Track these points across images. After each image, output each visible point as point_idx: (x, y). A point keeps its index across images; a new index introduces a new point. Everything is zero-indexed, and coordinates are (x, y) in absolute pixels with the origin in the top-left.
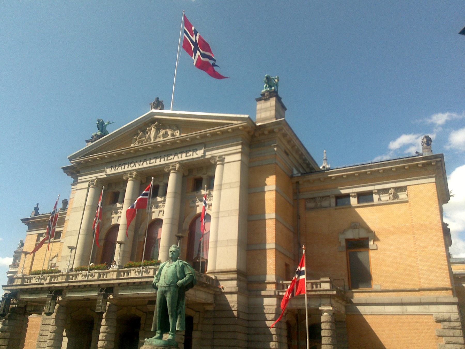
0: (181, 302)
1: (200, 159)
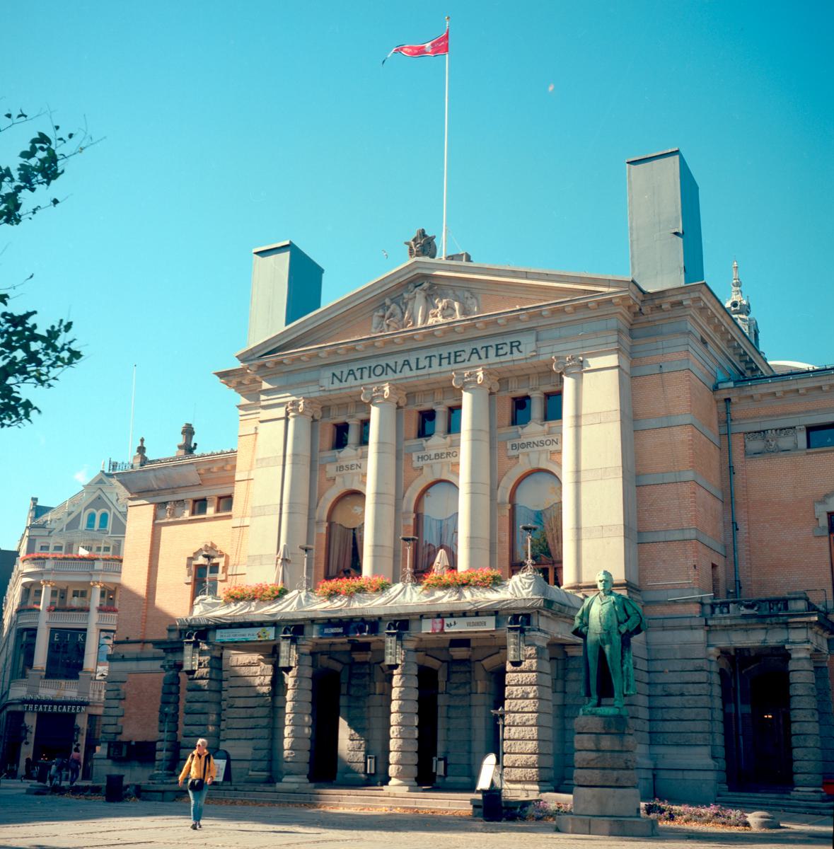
0: (626, 654)
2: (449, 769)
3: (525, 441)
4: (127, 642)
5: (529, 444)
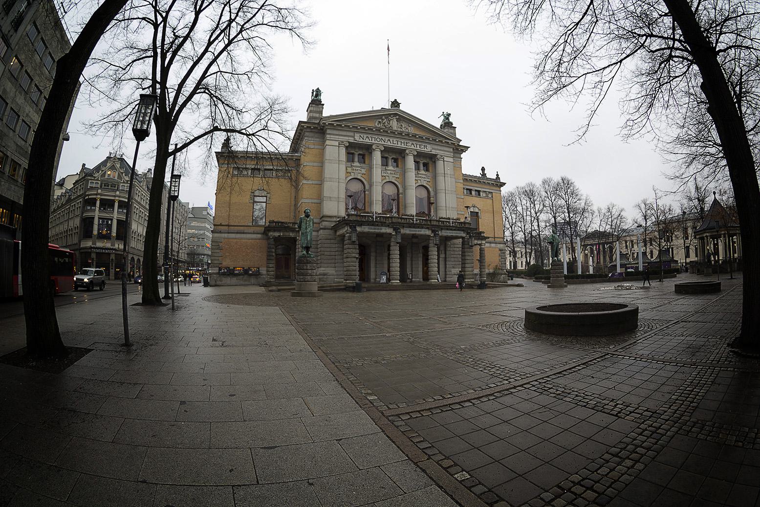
3: (420, 176)
4: (221, 225)
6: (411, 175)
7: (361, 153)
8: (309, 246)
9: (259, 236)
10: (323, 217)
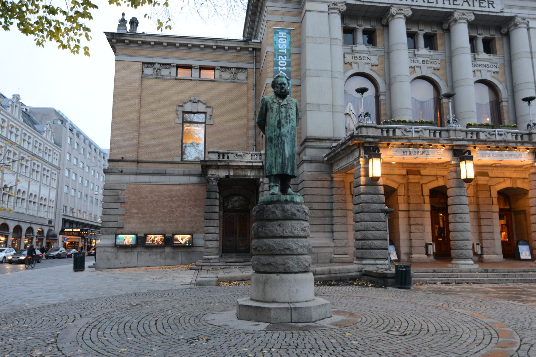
1: (498, 14)
2: (485, 249)
3: (478, 63)
4: (122, 160)
5: (480, 65)
6: (465, 61)
7: (368, 26)
8: (289, 172)
9: (194, 179)
10: (307, 140)
